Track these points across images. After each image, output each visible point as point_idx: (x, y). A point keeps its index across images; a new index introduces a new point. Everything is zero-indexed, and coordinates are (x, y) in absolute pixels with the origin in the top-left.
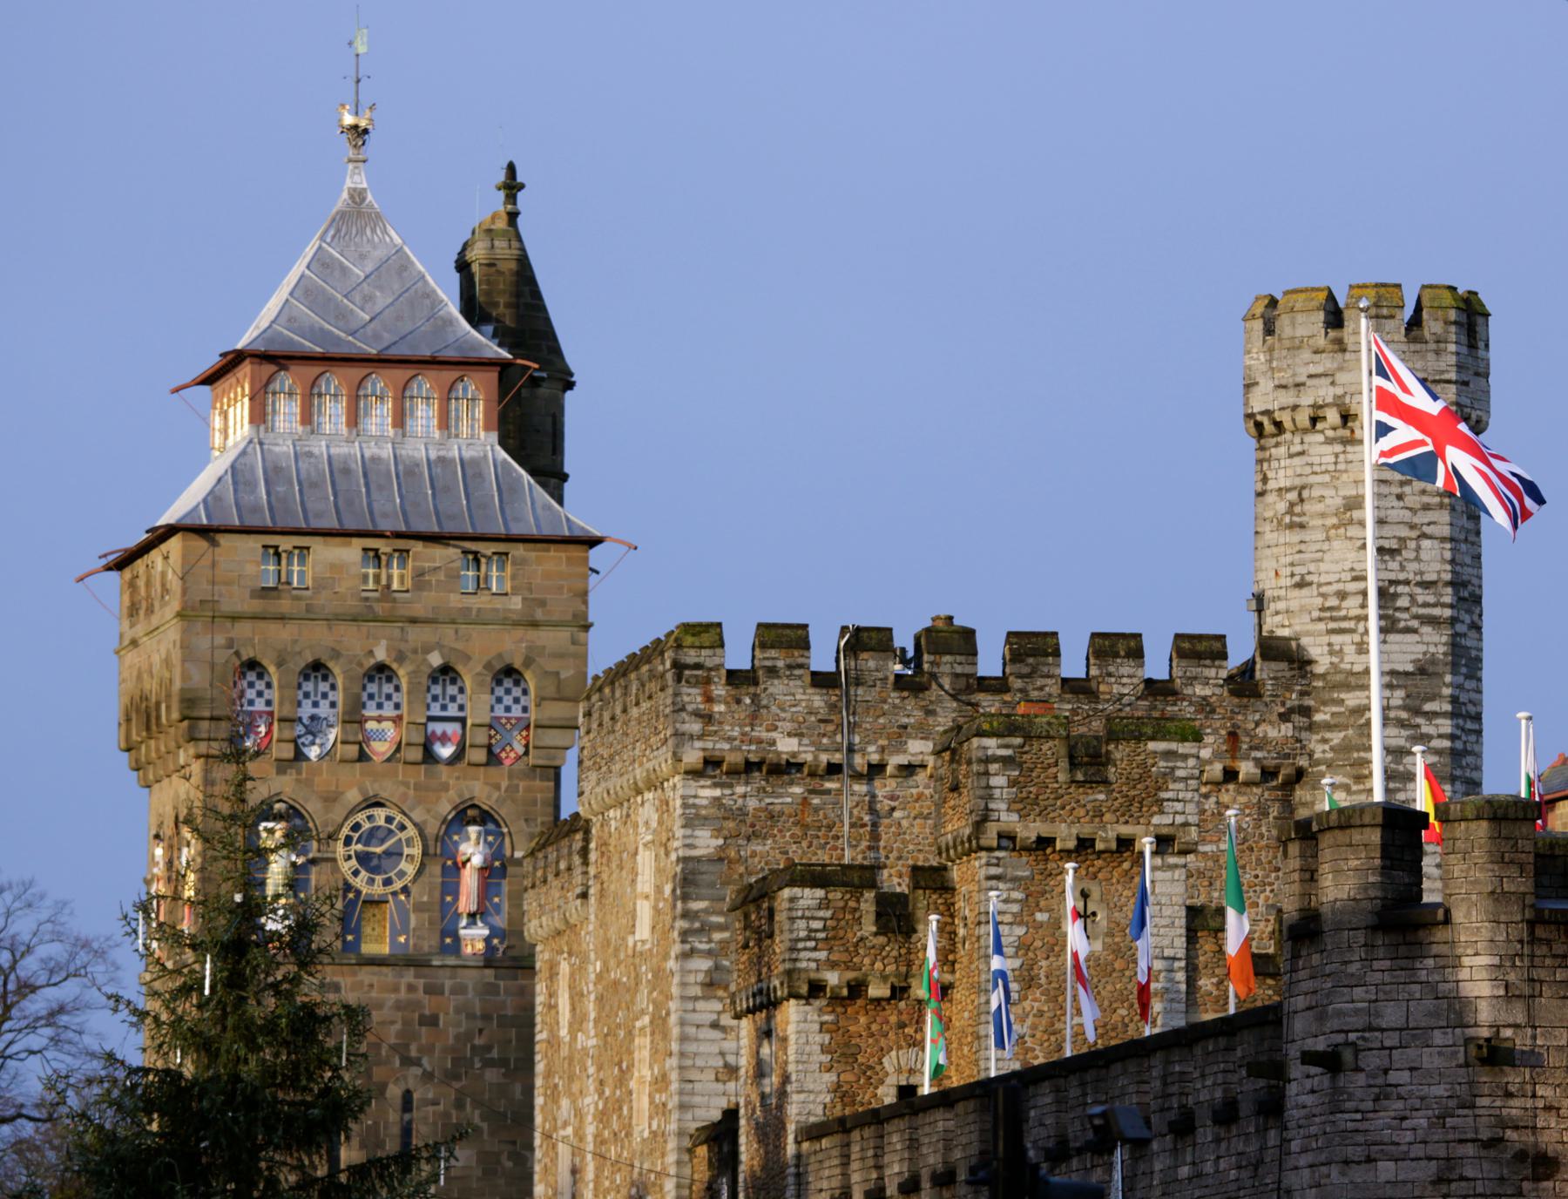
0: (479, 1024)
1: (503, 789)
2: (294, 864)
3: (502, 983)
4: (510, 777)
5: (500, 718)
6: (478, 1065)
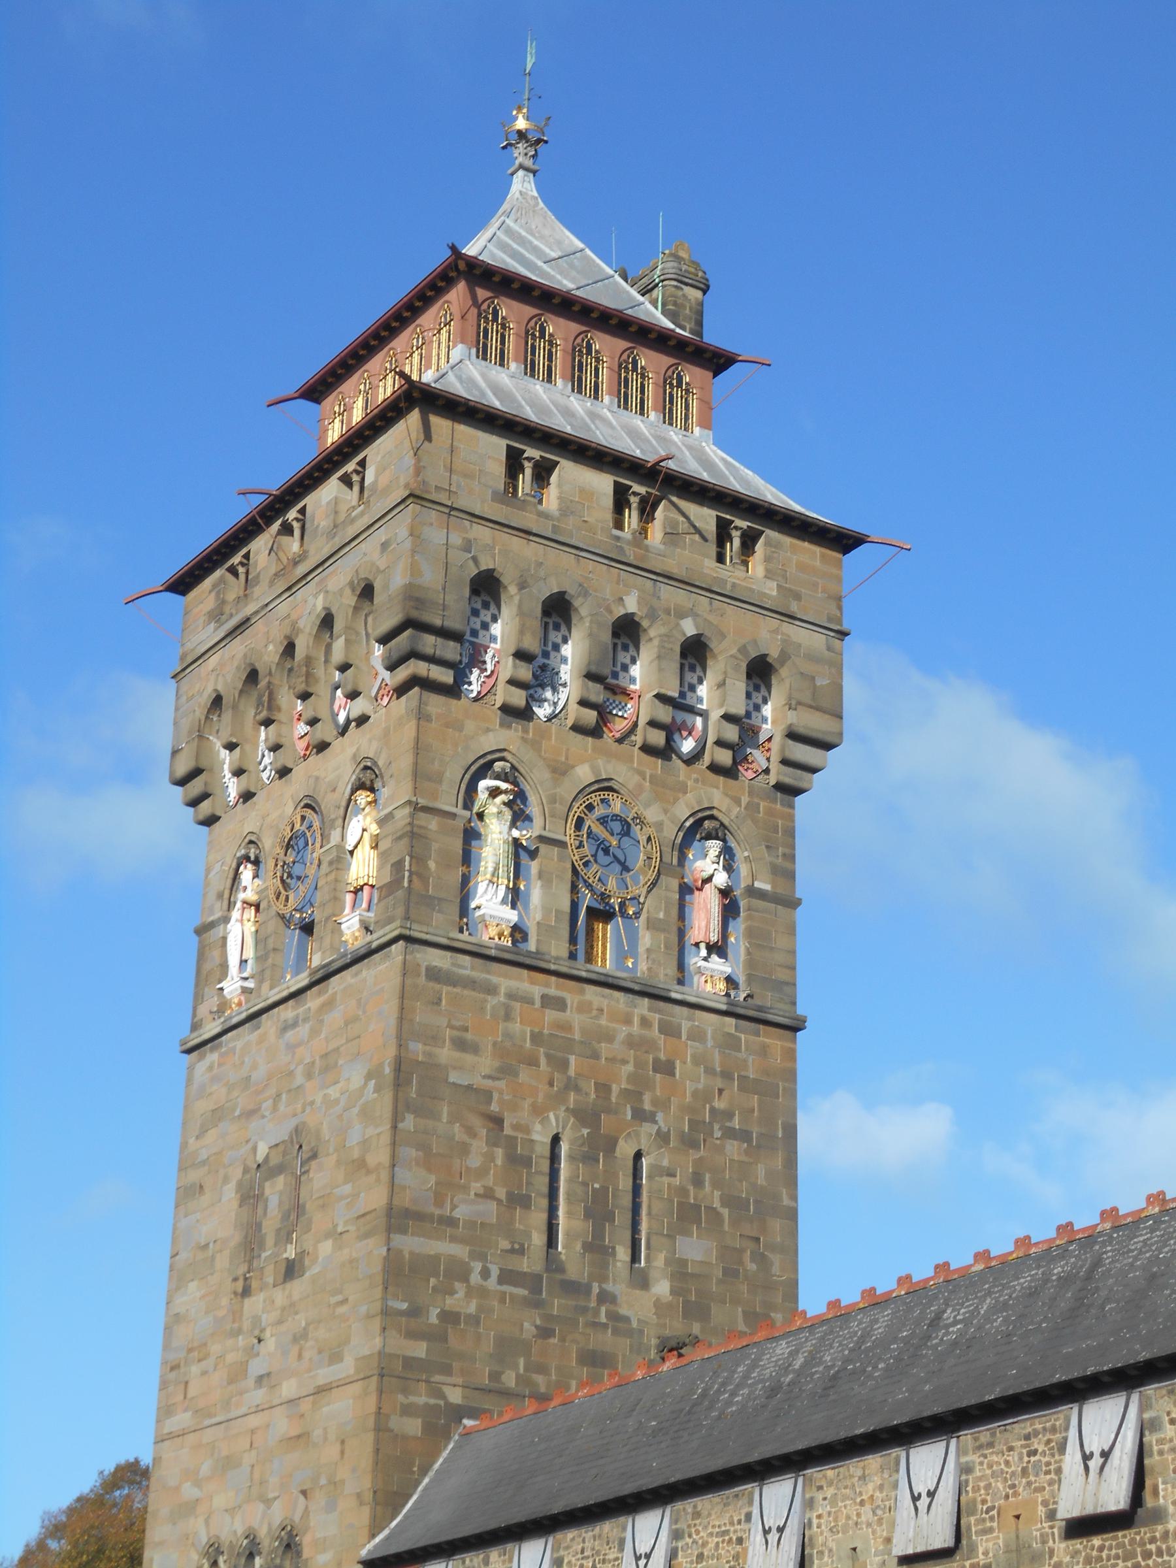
1: (743, 806)
2: (516, 840)
3: (743, 1036)
4: (751, 793)
6: (718, 1134)
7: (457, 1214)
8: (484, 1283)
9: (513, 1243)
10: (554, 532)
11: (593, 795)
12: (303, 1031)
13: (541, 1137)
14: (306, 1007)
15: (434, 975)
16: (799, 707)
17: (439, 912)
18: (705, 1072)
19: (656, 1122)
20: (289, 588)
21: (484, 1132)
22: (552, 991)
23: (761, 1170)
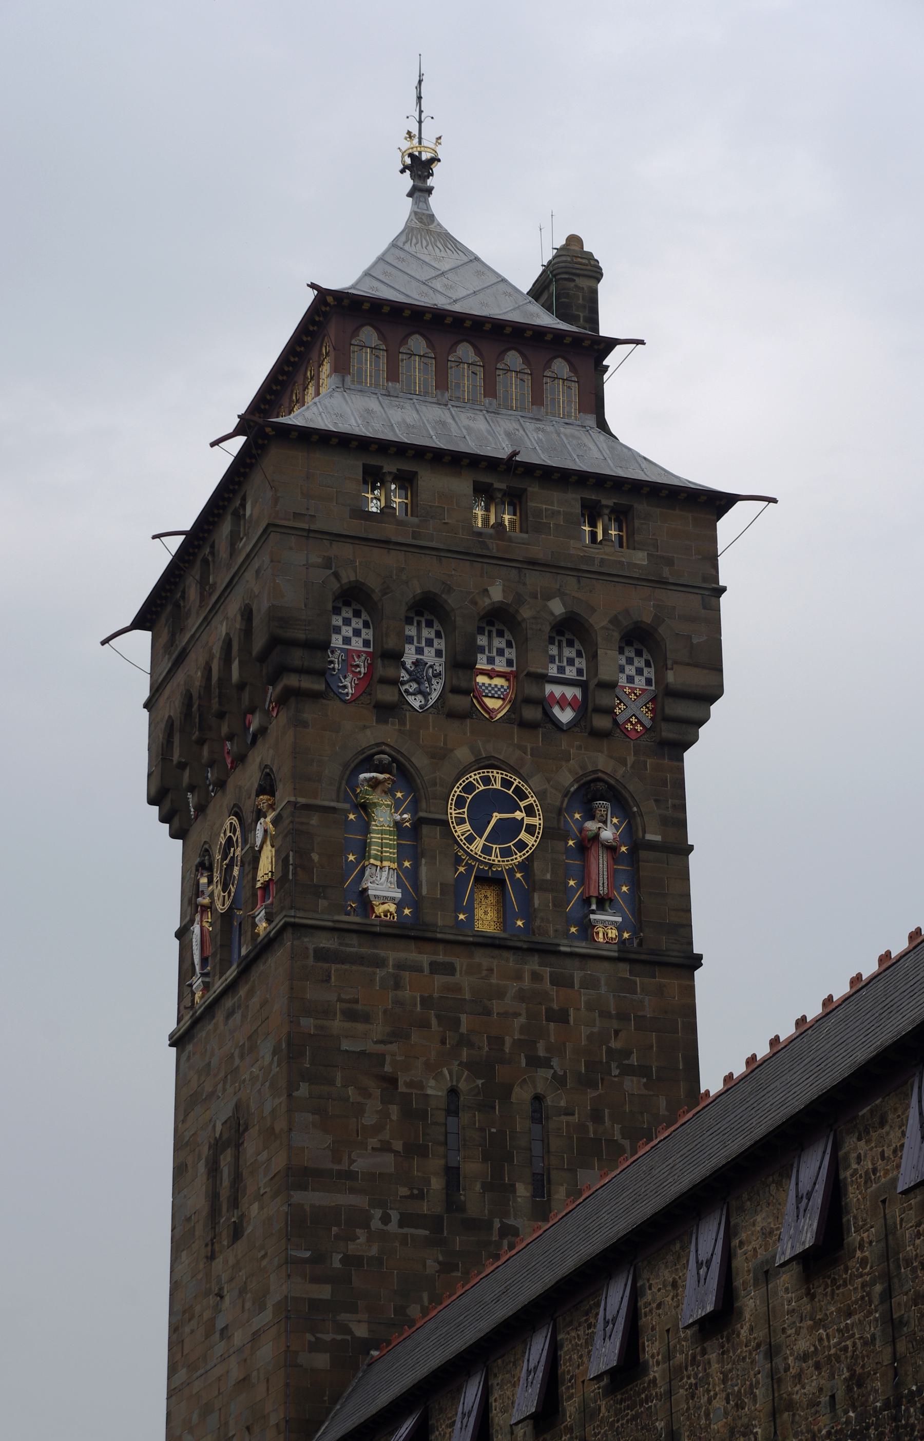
0: (615, 1024)
1: (629, 766)
2: (397, 824)
3: (638, 979)
5: (625, 687)
6: (616, 1072)
7: (354, 1167)
8: (385, 1228)
9: (411, 1189)
10: (414, 538)
11: (472, 774)
12: (238, 1016)
13: (435, 1090)
14: (239, 995)
15: (322, 955)
16: (675, 666)
17: (325, 898)
18: (599, 1016)
19: (552, 1067)
20: (205, 618)
21: (378, 1092)
22: (441, 958)
23: (662, 1102)
